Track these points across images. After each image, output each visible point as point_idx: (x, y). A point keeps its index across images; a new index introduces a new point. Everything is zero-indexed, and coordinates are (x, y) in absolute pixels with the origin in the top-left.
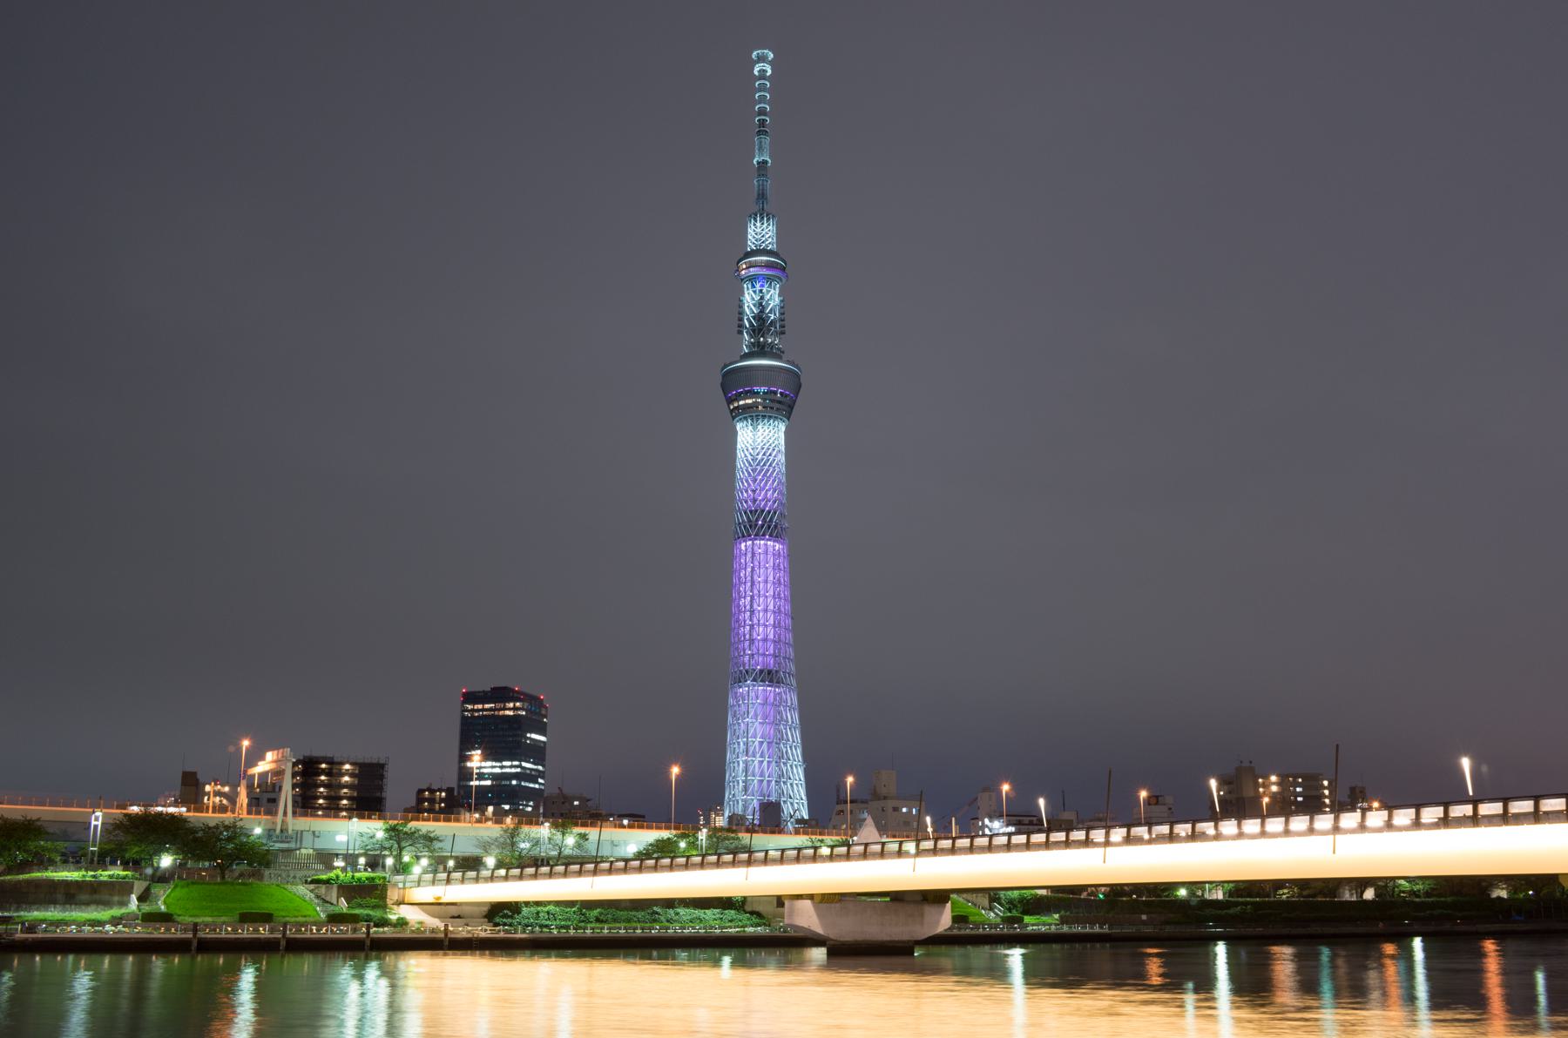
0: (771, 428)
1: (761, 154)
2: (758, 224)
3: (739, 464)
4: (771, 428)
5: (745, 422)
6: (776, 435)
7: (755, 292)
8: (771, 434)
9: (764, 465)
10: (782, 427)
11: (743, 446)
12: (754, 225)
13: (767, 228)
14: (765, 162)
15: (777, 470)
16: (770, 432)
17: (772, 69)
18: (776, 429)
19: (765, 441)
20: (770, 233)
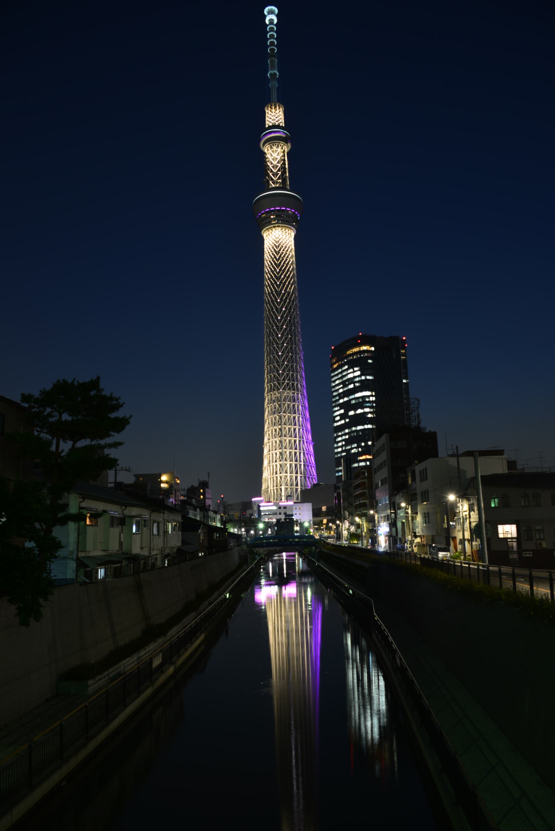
0: (287, 234)
1: (273, 68)
2: (273, 110)
3: (267, 256)
4: (287, 234)
5: (270, 231)
6: (290, 240)
7: (273, 151)
8: (287, 238)
9: (284, 256)
10: (293, 234)
11: (270, 246)
12: (271, 111)
13: (279, 113)
14: (275, 74)
15: (291, 260)
16: (286, 236)
17: (277, 19)
18: (290, 235)
19: (284, 242)
20: (281, 117)
